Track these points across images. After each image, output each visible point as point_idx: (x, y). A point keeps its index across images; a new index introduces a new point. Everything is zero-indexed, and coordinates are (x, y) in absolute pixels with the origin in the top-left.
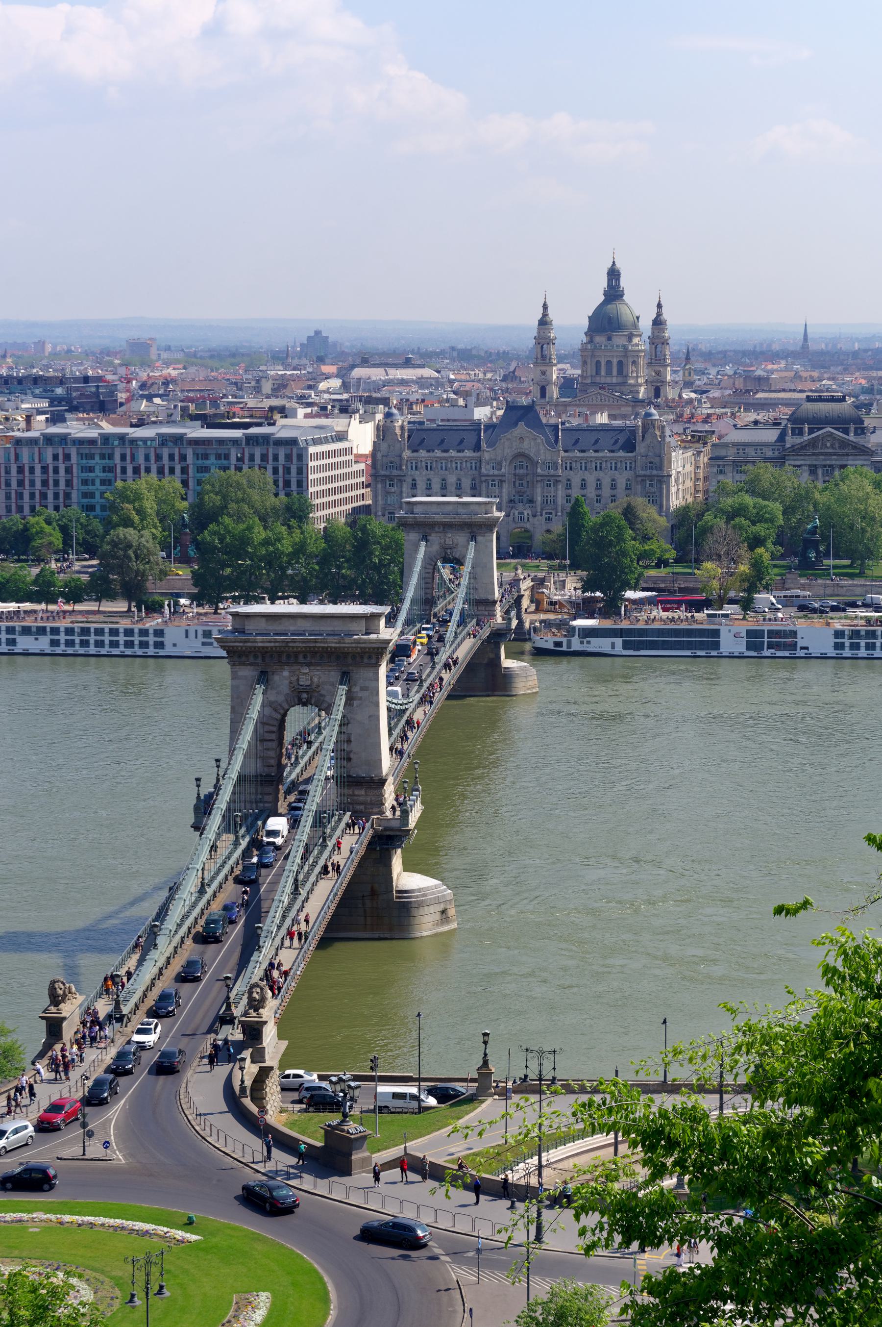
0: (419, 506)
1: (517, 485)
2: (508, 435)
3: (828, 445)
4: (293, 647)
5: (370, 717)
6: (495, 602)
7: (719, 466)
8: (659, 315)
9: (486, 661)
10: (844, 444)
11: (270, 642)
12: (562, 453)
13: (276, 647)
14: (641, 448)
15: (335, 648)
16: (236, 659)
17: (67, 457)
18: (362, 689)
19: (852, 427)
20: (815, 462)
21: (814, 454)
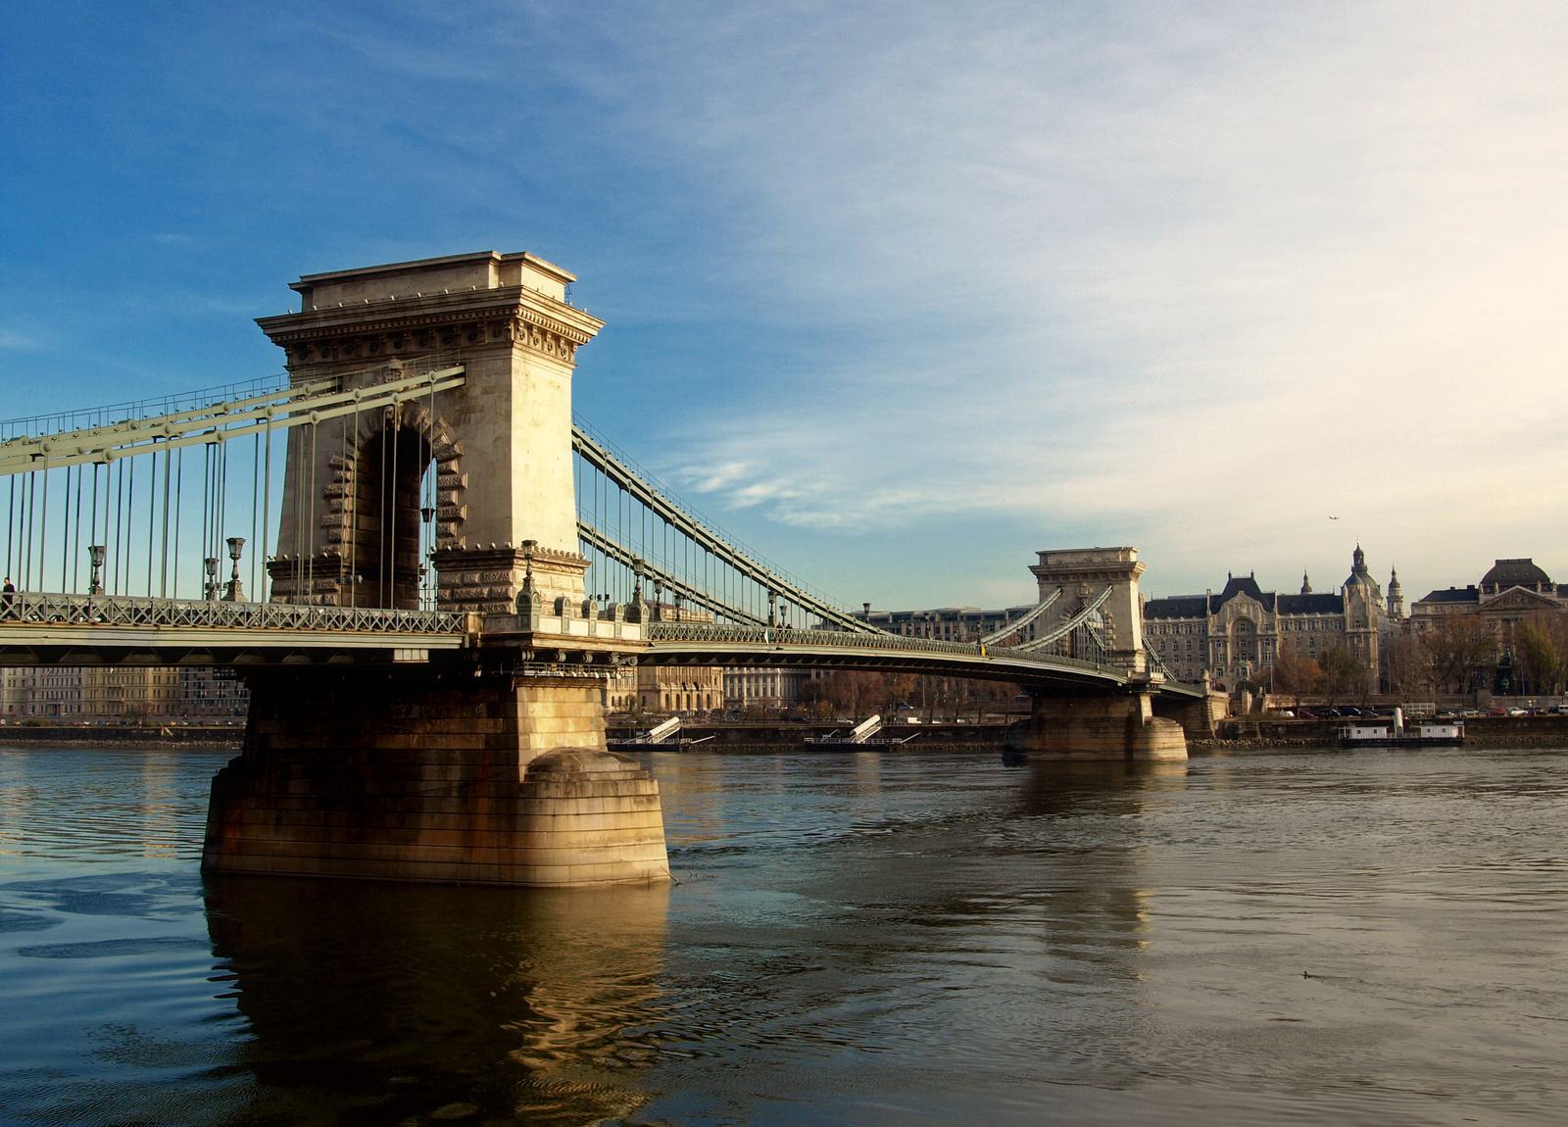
0: (1052, 557)
1: (1240, 644)
2: (1229, 602)
3: (1518, 600)
4: (373, 323)
5: (495, 441)
6: (1133, 653)
7: (1419, 623)
8: (1394, 580)
9: (1125, 715)
10: (1534, 599)
11: (336, 317)
12: (1278, 617)
13: (347, 326)
14: (1348, 609)
15: (436, 315)
16: (296, 362)
18: (485, 391)
19: (1539, 585)
20: (1506, 617)
21: (1505, 609)
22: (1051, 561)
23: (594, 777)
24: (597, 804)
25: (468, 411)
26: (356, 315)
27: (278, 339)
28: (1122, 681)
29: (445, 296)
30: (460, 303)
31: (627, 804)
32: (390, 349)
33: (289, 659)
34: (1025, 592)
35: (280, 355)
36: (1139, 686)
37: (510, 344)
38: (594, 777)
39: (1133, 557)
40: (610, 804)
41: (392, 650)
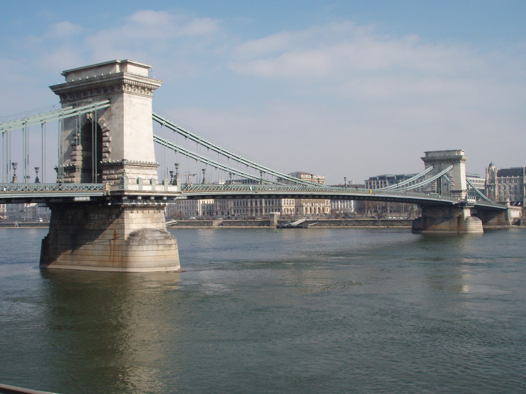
4: (82, 86)
6: (461, 191)
11: (72, 85)
15: (100, 83)
16: (63, 100)
17: (385, 183)
18: (116, 108)
22: (430, 156)
23: (149, 239)
24: (150, 247)
25: (111, 115)
26: (77, 84)
27: (57, 93)
28: (454, 202)
29: (101, 76)
30: (106, 78)
31: (161, 247)
32: (89, 95)
33: (52, 200)
34: (421, 169)
35: (58, 98)
36: (462, 205)
37: (122, 92)
38: (149, 239)
39: (462, 153)
40: (155, 247)
41: (74, 197)
